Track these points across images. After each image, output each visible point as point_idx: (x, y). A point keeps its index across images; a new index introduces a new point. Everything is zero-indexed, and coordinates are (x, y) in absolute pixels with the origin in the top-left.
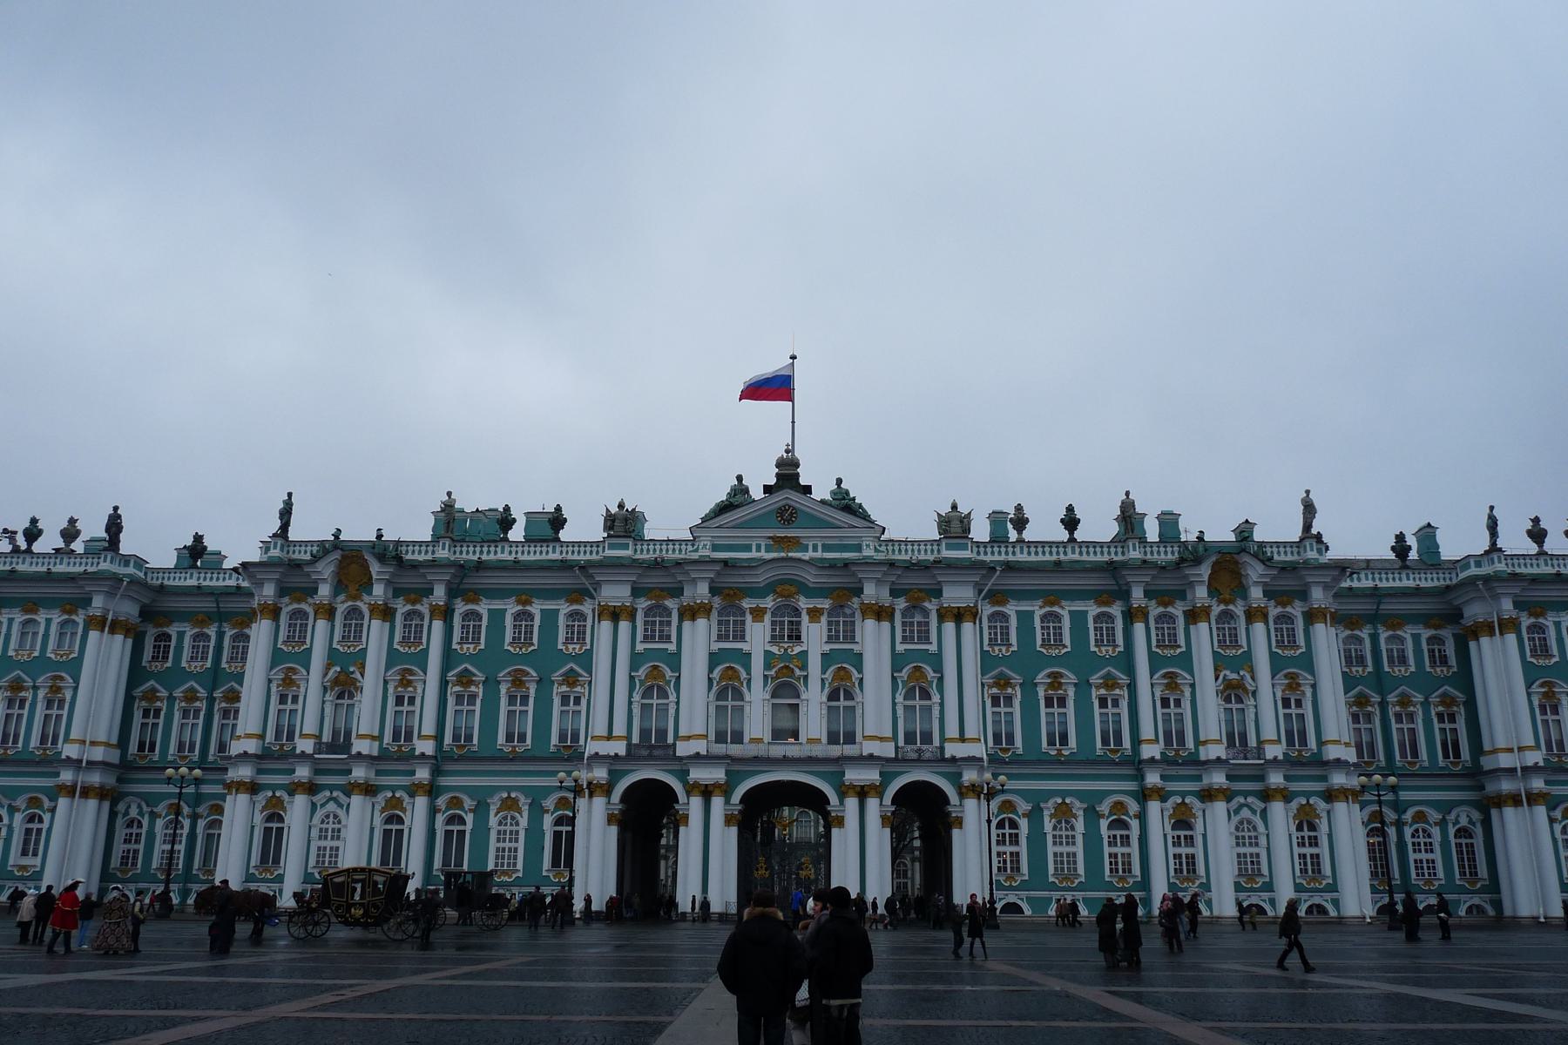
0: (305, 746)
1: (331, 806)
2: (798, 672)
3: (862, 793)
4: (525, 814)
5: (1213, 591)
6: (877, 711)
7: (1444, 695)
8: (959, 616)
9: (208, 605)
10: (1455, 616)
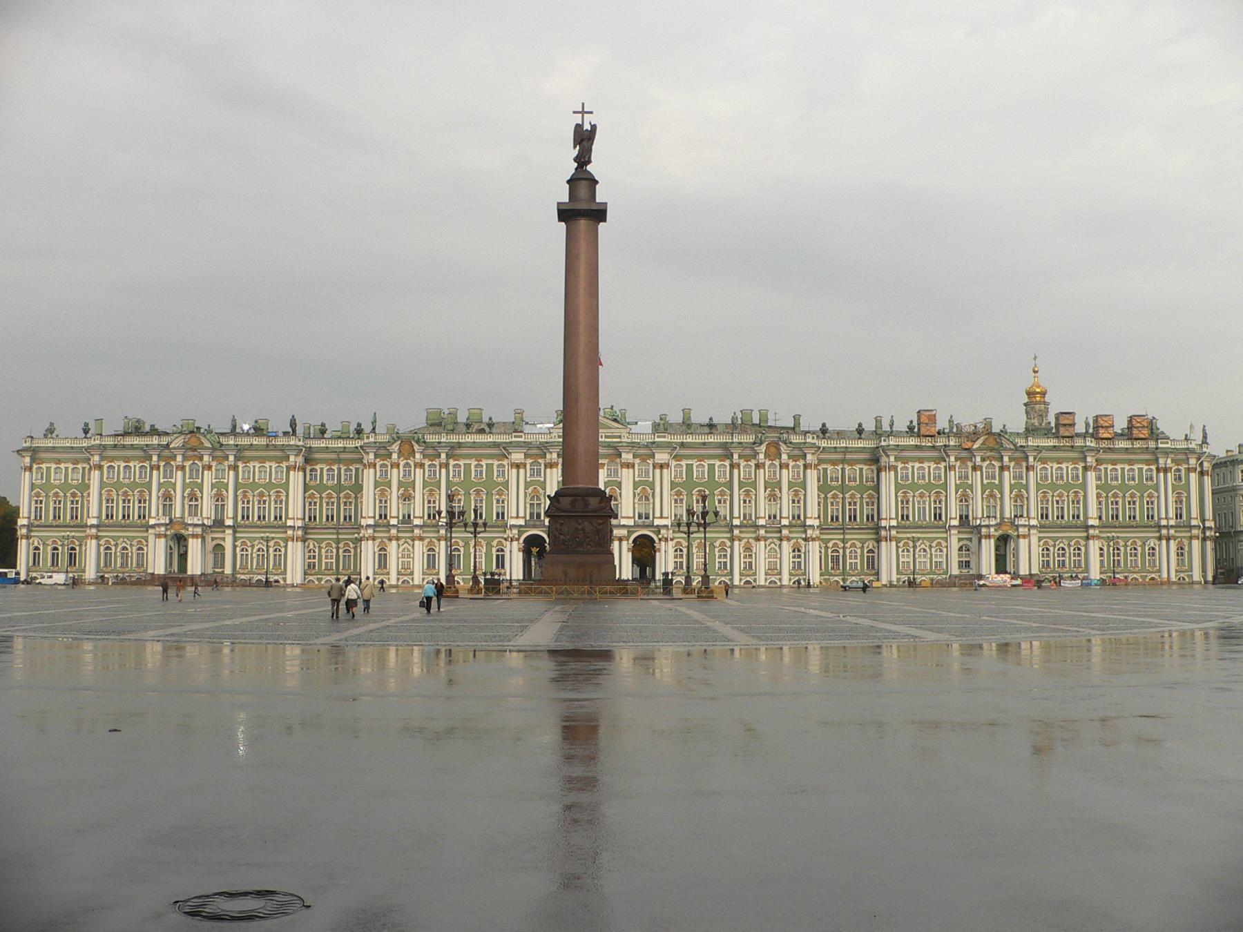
3: (620, 540)
5: (767, 455)
8: (661, 467)
9: (334, 456)
10: (876, 460)
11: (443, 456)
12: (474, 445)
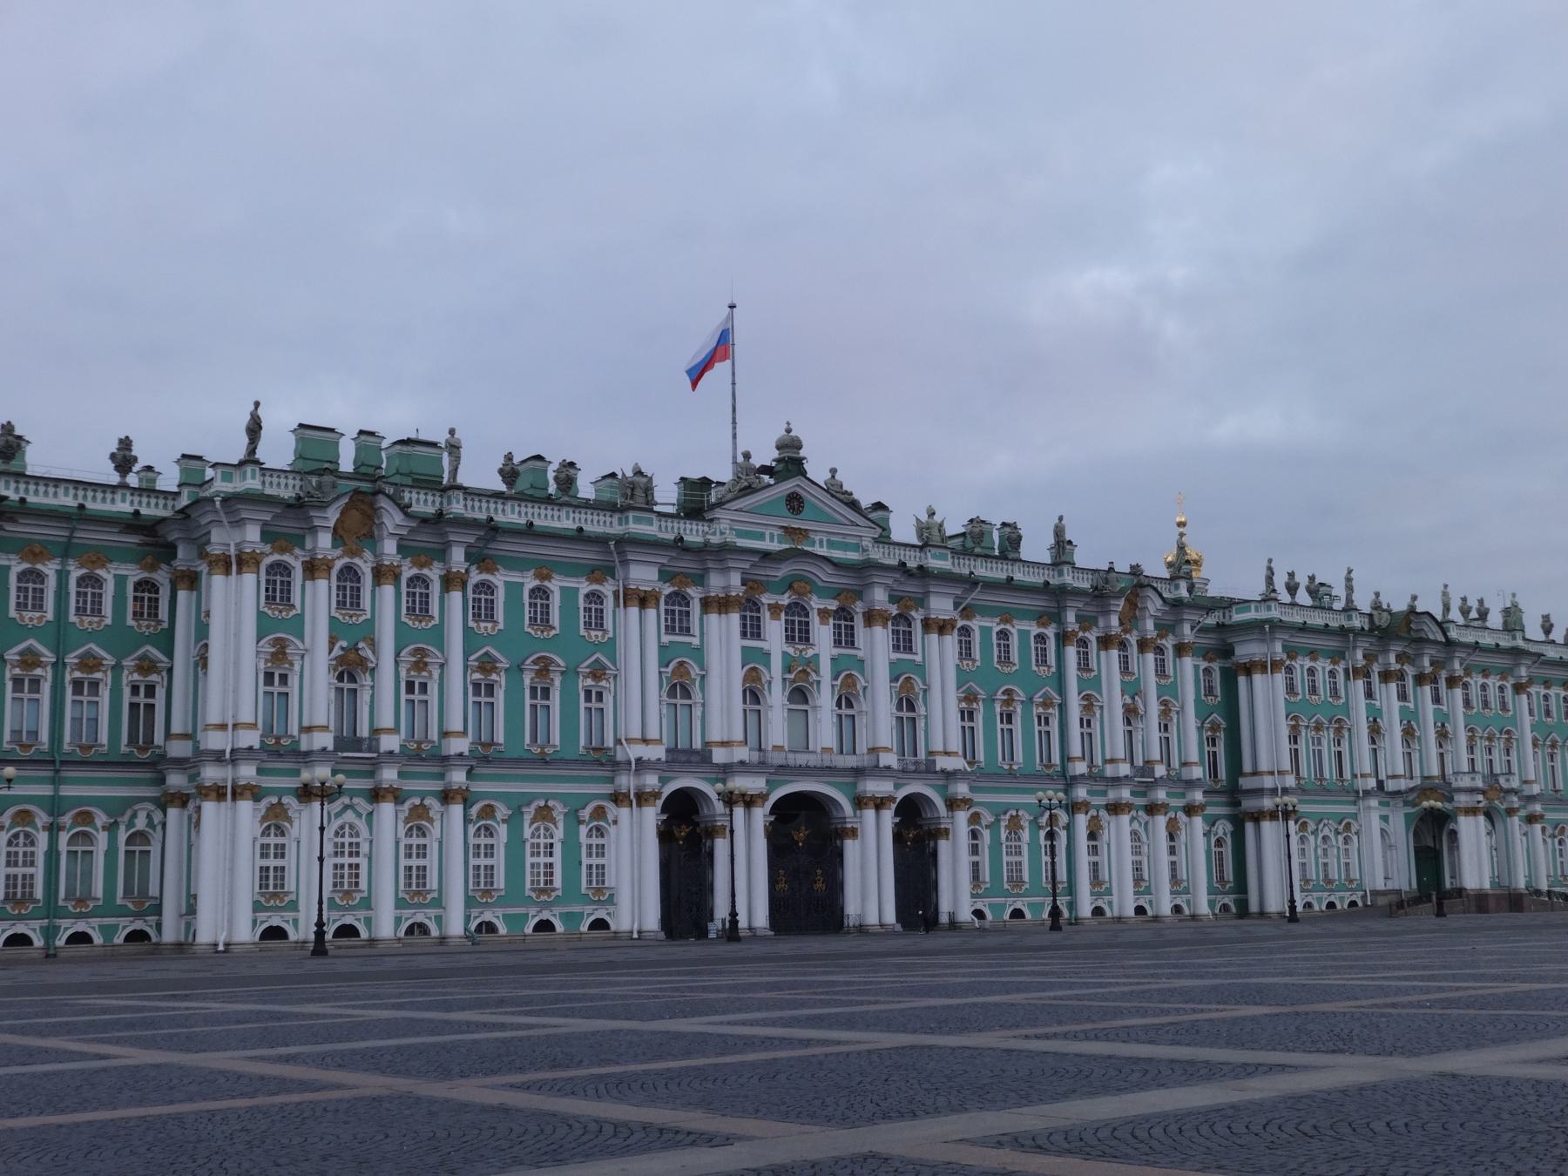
0: (325, 740)
1: (349, 816)
2: (814, 677)
3: (879, 804)
4: (561, 825)
5: (1121, 624)
6: (880, 722)
7: (1212, 722)
10: (1226, 652)
11: (458, 556)
12: (530, 531)
